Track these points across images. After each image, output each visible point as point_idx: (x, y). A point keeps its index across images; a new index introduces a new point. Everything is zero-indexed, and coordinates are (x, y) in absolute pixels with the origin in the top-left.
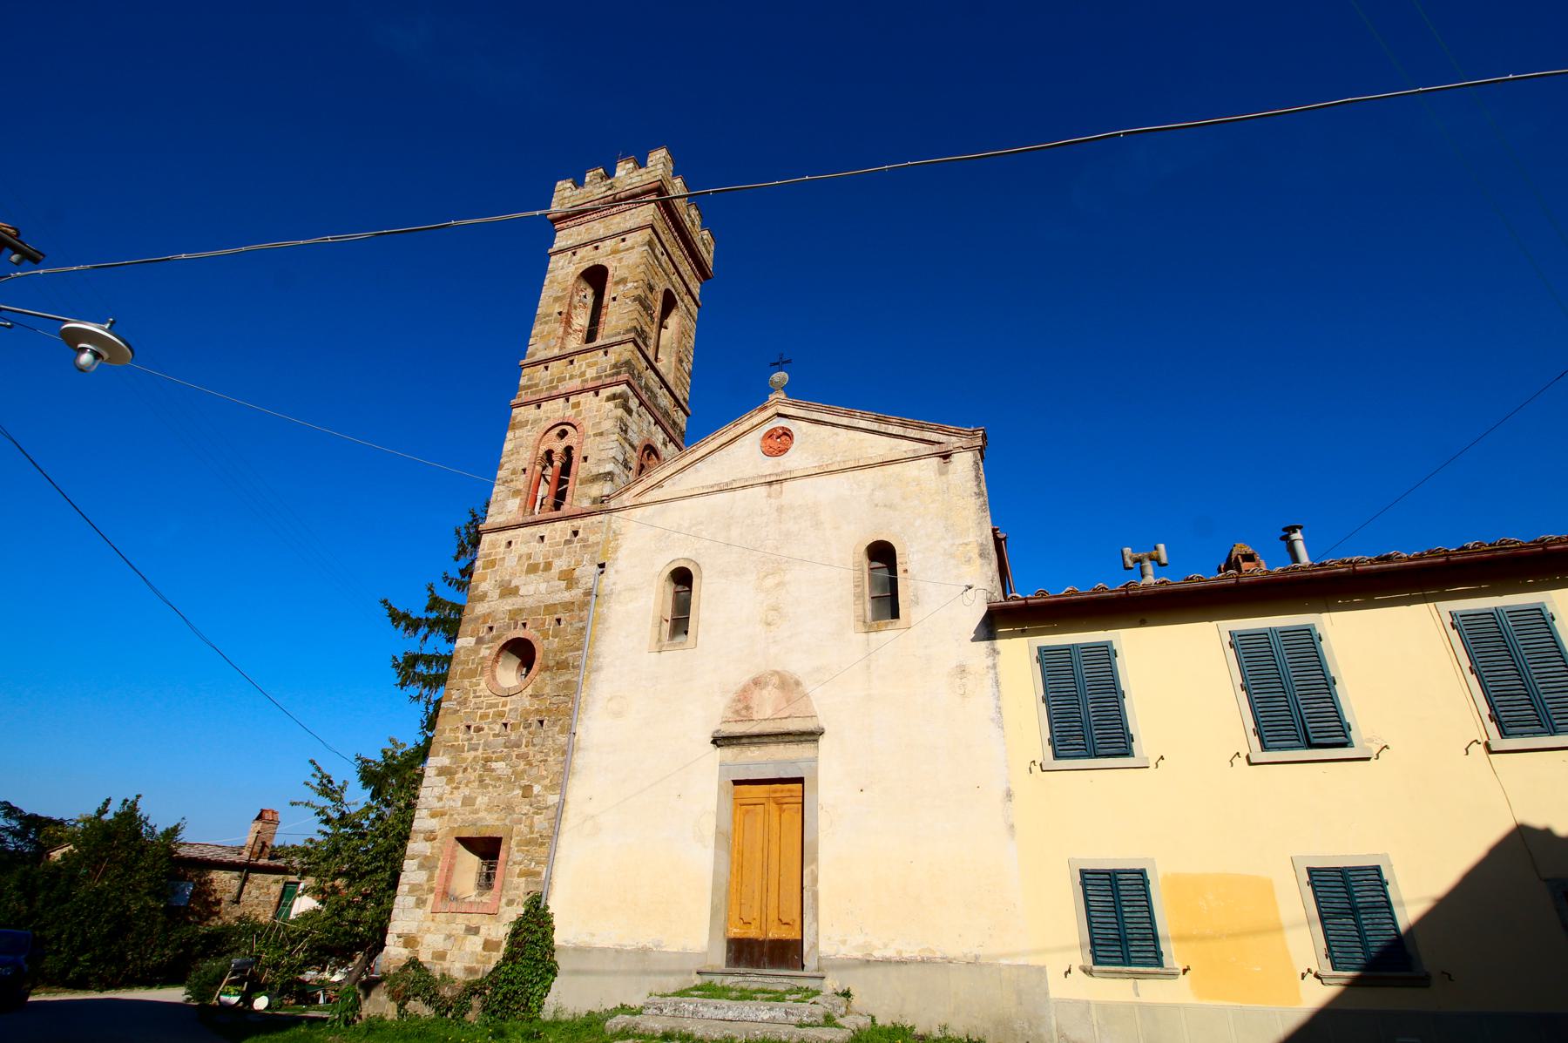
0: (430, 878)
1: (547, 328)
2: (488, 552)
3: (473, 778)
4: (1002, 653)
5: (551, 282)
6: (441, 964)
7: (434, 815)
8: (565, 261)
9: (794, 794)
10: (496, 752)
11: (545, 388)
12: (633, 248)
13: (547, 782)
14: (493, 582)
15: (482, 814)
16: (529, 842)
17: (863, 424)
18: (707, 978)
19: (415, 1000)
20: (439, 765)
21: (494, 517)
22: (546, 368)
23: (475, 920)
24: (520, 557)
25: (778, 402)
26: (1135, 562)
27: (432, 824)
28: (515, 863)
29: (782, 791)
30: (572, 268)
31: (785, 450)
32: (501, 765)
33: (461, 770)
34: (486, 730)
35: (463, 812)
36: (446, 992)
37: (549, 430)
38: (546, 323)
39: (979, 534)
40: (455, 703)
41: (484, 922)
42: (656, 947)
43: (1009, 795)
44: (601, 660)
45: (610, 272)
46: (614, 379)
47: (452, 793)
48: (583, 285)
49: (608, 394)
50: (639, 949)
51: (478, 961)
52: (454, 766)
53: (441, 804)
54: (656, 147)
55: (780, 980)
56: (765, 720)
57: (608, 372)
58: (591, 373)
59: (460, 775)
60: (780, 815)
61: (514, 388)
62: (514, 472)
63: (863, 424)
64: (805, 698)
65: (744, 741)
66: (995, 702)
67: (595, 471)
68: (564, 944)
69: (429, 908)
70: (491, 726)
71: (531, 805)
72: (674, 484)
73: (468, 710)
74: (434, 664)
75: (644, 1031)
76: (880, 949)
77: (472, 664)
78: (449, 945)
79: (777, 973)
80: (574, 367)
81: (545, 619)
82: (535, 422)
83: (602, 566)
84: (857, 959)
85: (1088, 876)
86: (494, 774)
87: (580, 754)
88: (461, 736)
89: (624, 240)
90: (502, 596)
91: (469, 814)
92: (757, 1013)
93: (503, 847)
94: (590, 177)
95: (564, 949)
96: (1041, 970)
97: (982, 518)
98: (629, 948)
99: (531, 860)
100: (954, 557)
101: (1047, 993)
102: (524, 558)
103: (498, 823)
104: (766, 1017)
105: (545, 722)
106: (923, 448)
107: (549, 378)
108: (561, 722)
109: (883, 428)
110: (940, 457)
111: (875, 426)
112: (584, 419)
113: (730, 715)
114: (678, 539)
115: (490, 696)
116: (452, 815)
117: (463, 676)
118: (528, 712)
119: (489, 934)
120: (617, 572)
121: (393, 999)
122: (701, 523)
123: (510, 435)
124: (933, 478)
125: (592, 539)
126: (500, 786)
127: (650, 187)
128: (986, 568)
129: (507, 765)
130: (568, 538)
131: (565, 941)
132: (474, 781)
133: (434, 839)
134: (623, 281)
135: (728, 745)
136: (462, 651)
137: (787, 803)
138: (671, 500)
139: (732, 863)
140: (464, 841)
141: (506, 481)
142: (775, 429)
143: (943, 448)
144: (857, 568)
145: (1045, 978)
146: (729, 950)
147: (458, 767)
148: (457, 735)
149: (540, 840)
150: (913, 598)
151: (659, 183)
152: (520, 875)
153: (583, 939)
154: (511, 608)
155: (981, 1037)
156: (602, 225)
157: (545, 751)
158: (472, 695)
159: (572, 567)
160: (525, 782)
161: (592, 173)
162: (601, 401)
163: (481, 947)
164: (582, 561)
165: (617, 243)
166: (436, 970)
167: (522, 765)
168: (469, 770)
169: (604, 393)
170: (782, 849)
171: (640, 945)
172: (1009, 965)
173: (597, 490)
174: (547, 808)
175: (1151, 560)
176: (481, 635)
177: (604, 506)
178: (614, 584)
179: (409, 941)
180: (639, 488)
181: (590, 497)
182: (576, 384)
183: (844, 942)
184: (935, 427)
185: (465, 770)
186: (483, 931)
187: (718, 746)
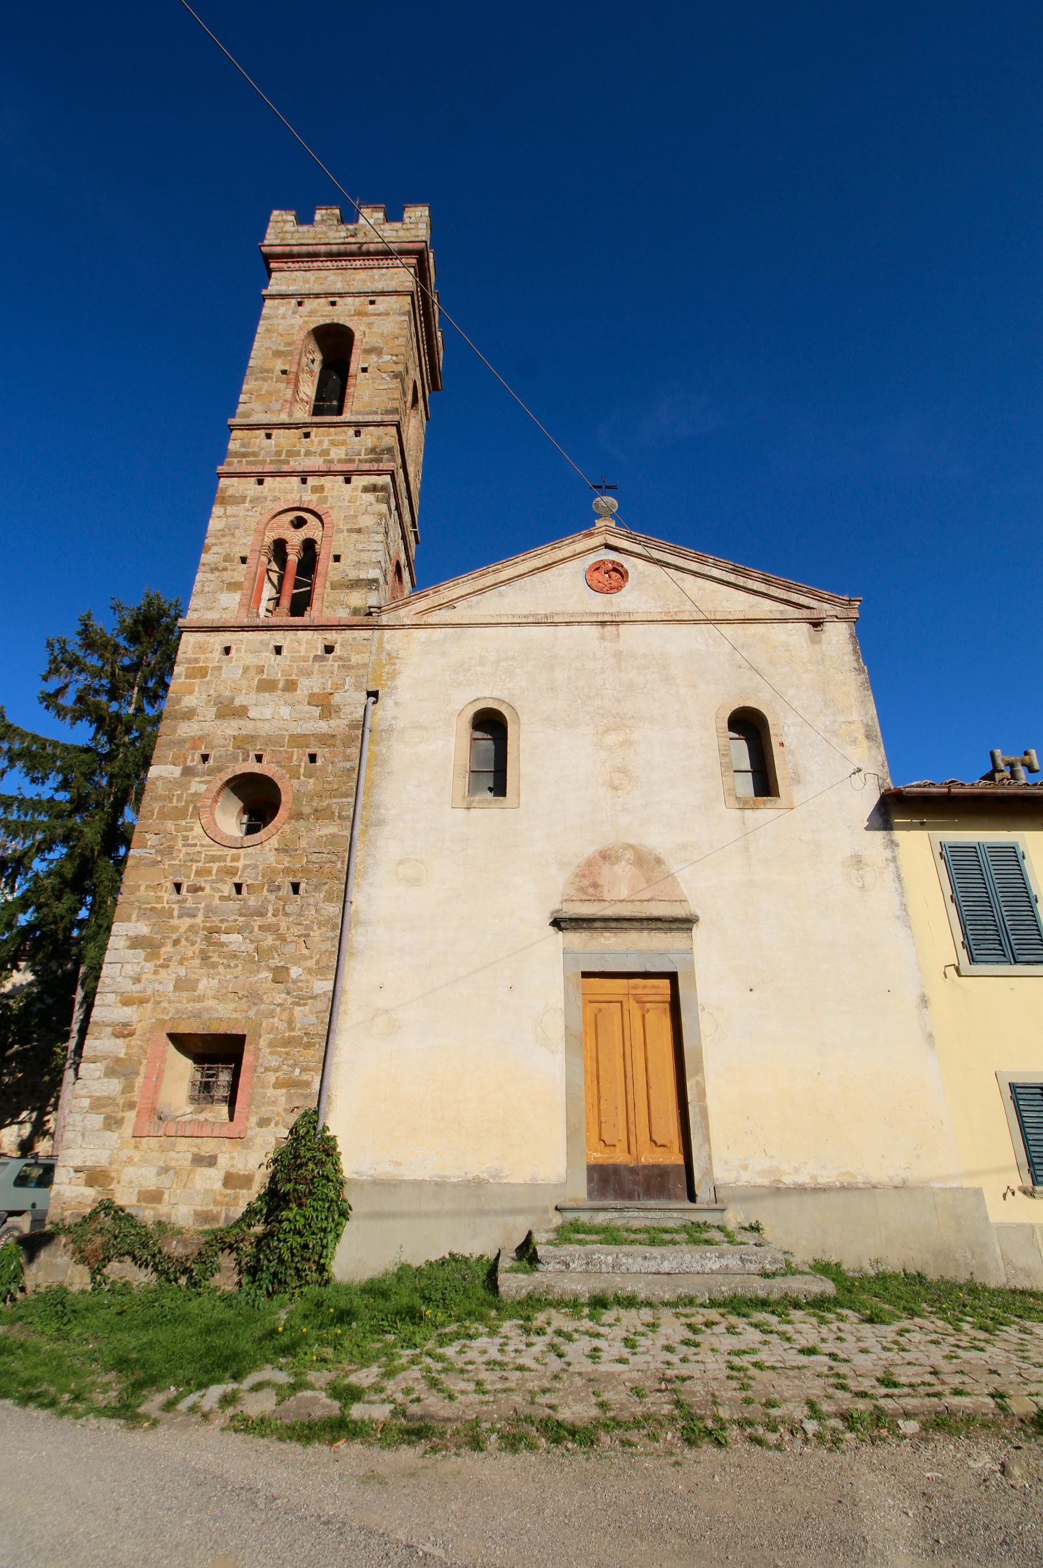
0: (128, 1088)
1: (266, 387)
2: (193, 656)
3: (191, 954)
4: (901, 845)
5: (267, 330)
6: (153, 1209)
7: (127, 1002)
8: (287, 309)
9: (660, 991)
10: (227, 921)
11: (268, 460)
12: (387, 314)
13: (311, 963)
14: (204, 696)
15: (210, 1003)
16: (288, 1042)
17: (716, 573)
18: (570, 1216)
19: (120, 1262)
20: (131, 934)
21: (197, 611)
22: (269, 436)
23: (208, 1147)
24: (246, 669)
25: (605, 530)
26: (1006, 765)
27: (128, 1013)
28: (267, 1069)
29: (644, 987)
30: (298, 321)
31: (619, 588)
32: (235, 937)
33: (170, 942)
34: (208, 890)
35: (176, 999)
36: (175, 1248)
37: (280, 513)
38: (264, 379)
39: (863, 713)
40: (153, 851)
41: (224, 1149)
42: (494, 1177)
43: (924, 1001)
44: (382, 811)
45: (358, 336)
46: (375, 466)
47: (156, 972)
48: (313, 346)
49: (365, 483)
50: (469, 1181)
51: (216, 1203)
52: (159, 936)
53: (138, 987)
54: (417, 201)
55: (669, 1214)
56: (621, 901)
57: (363, 457)
58: (337, 454)
59: (168, 949)
60: (644, 1016)
61: (221, 453)
62: (227, 558)
63: (716, 573)
64: (670, 878)
65: (597, 924)
66: (899, 898)
67: (353, 574)
68: (355, 1176)
69: (128, 1130)
70: (215, 885)
71: (288, 993)
72: (470, 607)
73: (177, 862)
74: (15, 808)
75: (561, 1295)
76: (790, 1174)
77: (178, 801)
78: (165, 1181)
79: (665, 1207)
80: (312, 442)
81: (292, 752)
82: (256, 500)
83: (374, 694)
84: (763, 1186)
85: (1018, 1090)
86: (225, 949)
87: (360, 930)
88: (166, 896)
89: (372, 303)
90: (221, 715)
91: (188, 1002)
92: (703, 1262)
93: (248, 1048)
94: (322, 216)
95: (358, 1183)
96: (978, 1193)
97: (865, 696)
98: (453, 1180)
99: (294, 1066)
100: (837, 736)
101: (987, 1218)
102: (252, 672)
103: (235, 1015)
104: (716, 1267)
105: (302, 886)
106: (791, 612)
107: (273, 449)
108: (326, 887)
109: (741, 581)
110: (810, 623)
111: (731, 578)
112: (331, 508)
113: (572, 892)
114: (482, 674)
115: (212, 846)
116: (159, 1003)
117: (164, 816)
118: (274, 871)
119: (232, 1166)
120: (396, 703)
121: (84, 1260)
122: (513, 658)
123: (217, 510)
124: (805, 645)
125: (355, 659)
126: (236, 966)
127: (410, 246)
128: (874, 752)
129: (245, 938)
130: (319, 653)
131: (357, 1173)
132: (192, 958)
133: (131, 1034)
134: (377, 351)
135: (575, 929)
136: (159, 783)
137: (650, 1002)
138: (469, 625)
139: (586, 1072)
140: (181, 1041)
141: (217, 569)
142: (603, 562)
143: (815, 614)
144: (722, 735)
145: (983, 1199)
146: (590, 1180)
147: (164, 938)
148: (159, 894)
149: (305, 1039)
150: (793, 775)
151: (423, 244)
152: (277, 1085)
153: (385, 1170)
154: (236, 733)
155: (920, 1270)
156: (340, 278)
157: (305, 923)
158: (180, 843)
159: (329, 691)
160: (275, 962)
161: (324, 212)
162: (355, 489)
163: (220, 1183)
164: (343, 685)
165: (363, 304)
166: (147, 1215)
167: (269, 940)
168: (183, 942)
169: (358, 481)
170: (649, 1056)
171: (470, 1176)
172: (942, 1189)
173: (358, 599)
174: (314, 998)
175: (1023, 765)
176: (189, 763)
177: (371, 620)
178: (395, 718)
179: (95, 1177)
180: (423, 604)
181: (348, 607)
182: (316, 463)
183: (745, 1167)
184: (805, 590)
185: (176, 942)
186: (223, 1161)
187: (561, 929)
